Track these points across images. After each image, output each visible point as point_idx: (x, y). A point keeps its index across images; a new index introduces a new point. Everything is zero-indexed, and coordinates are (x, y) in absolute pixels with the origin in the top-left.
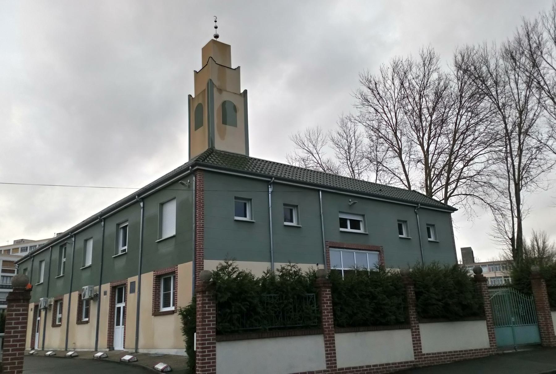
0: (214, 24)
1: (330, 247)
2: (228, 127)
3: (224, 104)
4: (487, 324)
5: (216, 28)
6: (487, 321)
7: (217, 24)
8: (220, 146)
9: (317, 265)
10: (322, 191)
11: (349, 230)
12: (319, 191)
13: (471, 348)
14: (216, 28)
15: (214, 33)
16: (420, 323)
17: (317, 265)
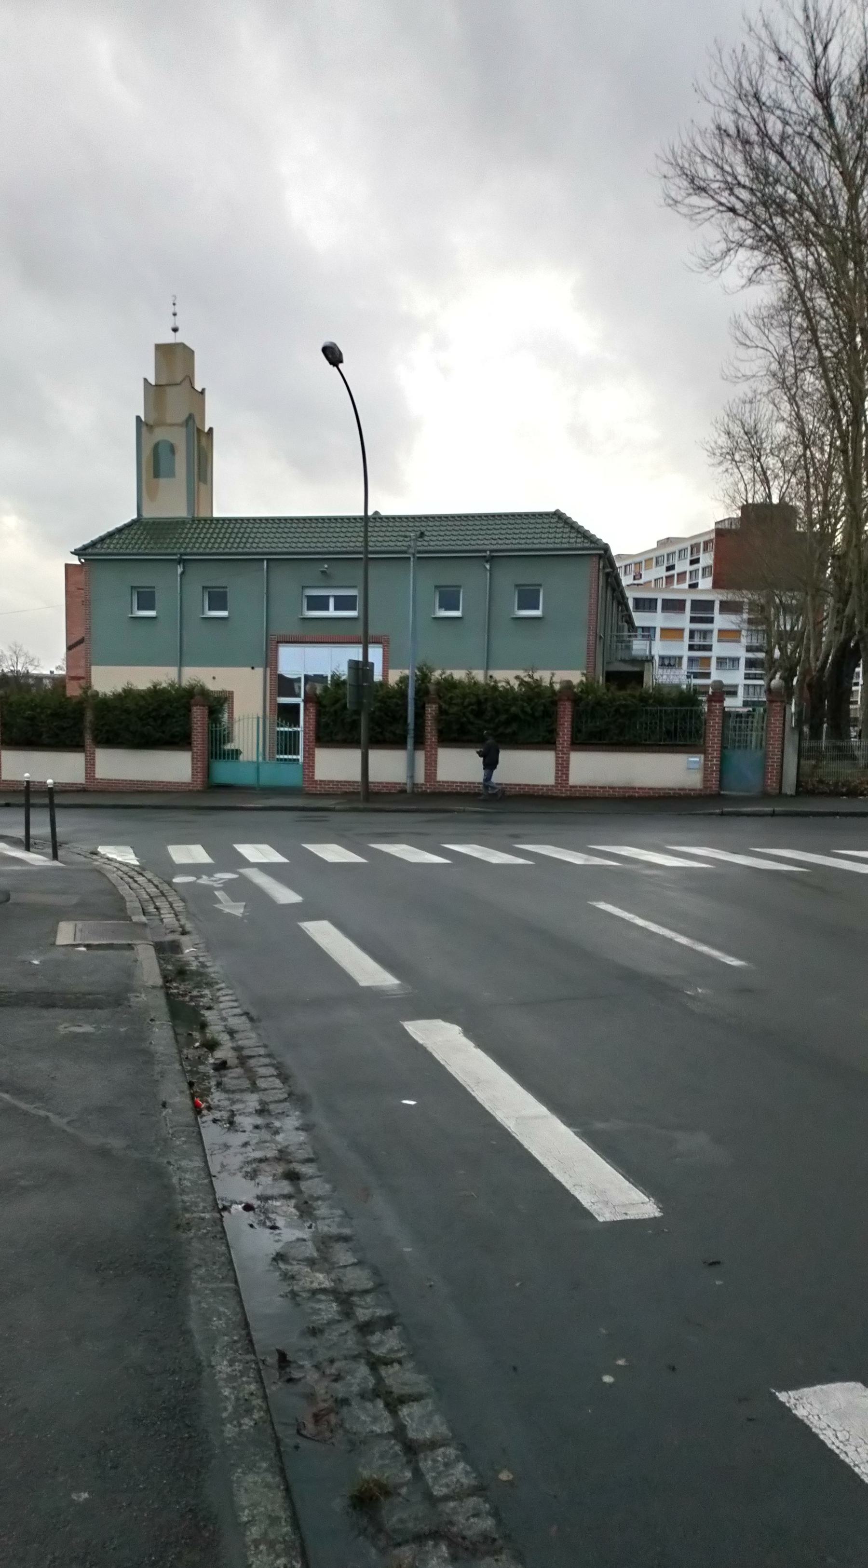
0: (172, 309)
1: (278, 642)
2: (162, 481)
3: (156, 447)
4: (193, 755)
5: (175, 314)
6: (193, 753)
7: (177, 309)
8: (146, 515)
9: (253, 668)
10: (268, 560)
11: (332, 613)
12: (262, 560)
13: (160, 779)
14: (175, 314)
15: (172, 325)
16: (98, 747)
17: (253, 668)
